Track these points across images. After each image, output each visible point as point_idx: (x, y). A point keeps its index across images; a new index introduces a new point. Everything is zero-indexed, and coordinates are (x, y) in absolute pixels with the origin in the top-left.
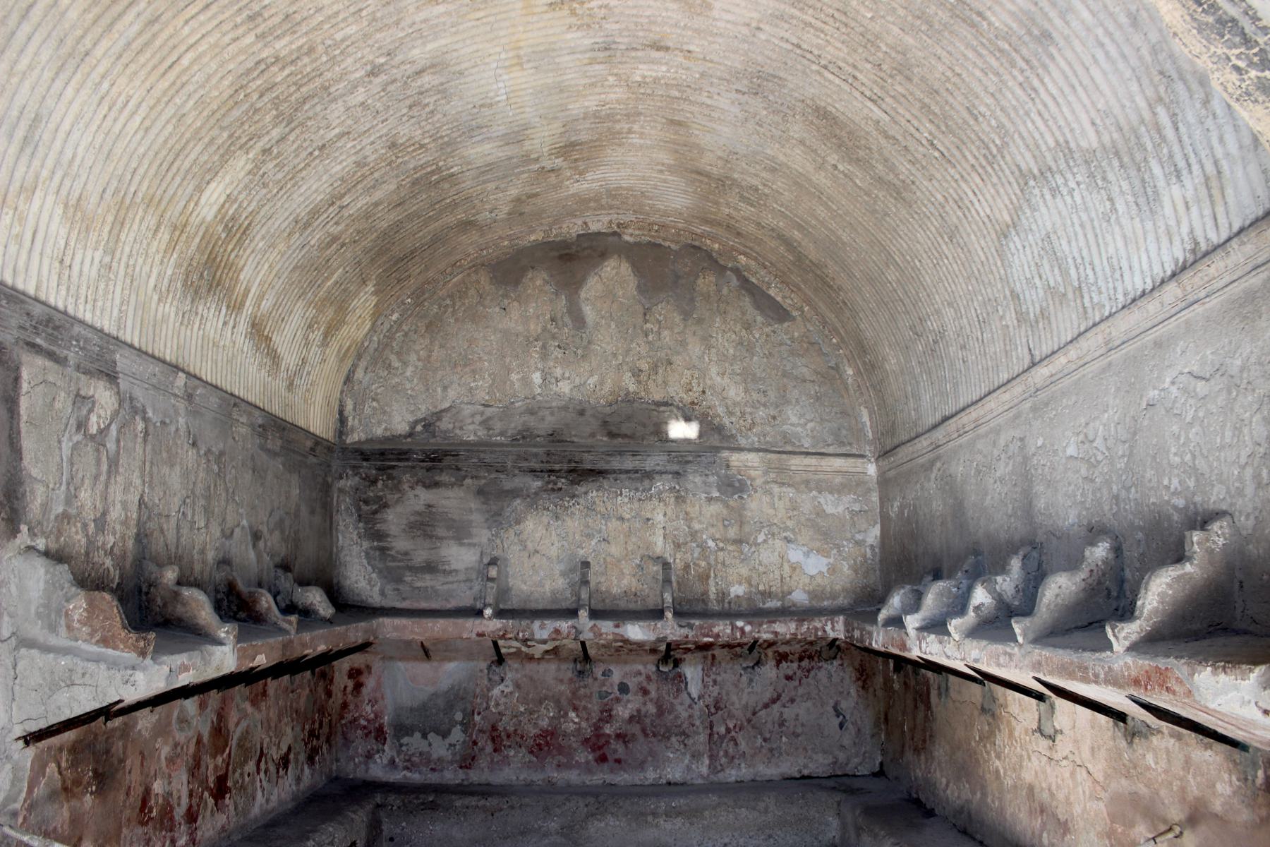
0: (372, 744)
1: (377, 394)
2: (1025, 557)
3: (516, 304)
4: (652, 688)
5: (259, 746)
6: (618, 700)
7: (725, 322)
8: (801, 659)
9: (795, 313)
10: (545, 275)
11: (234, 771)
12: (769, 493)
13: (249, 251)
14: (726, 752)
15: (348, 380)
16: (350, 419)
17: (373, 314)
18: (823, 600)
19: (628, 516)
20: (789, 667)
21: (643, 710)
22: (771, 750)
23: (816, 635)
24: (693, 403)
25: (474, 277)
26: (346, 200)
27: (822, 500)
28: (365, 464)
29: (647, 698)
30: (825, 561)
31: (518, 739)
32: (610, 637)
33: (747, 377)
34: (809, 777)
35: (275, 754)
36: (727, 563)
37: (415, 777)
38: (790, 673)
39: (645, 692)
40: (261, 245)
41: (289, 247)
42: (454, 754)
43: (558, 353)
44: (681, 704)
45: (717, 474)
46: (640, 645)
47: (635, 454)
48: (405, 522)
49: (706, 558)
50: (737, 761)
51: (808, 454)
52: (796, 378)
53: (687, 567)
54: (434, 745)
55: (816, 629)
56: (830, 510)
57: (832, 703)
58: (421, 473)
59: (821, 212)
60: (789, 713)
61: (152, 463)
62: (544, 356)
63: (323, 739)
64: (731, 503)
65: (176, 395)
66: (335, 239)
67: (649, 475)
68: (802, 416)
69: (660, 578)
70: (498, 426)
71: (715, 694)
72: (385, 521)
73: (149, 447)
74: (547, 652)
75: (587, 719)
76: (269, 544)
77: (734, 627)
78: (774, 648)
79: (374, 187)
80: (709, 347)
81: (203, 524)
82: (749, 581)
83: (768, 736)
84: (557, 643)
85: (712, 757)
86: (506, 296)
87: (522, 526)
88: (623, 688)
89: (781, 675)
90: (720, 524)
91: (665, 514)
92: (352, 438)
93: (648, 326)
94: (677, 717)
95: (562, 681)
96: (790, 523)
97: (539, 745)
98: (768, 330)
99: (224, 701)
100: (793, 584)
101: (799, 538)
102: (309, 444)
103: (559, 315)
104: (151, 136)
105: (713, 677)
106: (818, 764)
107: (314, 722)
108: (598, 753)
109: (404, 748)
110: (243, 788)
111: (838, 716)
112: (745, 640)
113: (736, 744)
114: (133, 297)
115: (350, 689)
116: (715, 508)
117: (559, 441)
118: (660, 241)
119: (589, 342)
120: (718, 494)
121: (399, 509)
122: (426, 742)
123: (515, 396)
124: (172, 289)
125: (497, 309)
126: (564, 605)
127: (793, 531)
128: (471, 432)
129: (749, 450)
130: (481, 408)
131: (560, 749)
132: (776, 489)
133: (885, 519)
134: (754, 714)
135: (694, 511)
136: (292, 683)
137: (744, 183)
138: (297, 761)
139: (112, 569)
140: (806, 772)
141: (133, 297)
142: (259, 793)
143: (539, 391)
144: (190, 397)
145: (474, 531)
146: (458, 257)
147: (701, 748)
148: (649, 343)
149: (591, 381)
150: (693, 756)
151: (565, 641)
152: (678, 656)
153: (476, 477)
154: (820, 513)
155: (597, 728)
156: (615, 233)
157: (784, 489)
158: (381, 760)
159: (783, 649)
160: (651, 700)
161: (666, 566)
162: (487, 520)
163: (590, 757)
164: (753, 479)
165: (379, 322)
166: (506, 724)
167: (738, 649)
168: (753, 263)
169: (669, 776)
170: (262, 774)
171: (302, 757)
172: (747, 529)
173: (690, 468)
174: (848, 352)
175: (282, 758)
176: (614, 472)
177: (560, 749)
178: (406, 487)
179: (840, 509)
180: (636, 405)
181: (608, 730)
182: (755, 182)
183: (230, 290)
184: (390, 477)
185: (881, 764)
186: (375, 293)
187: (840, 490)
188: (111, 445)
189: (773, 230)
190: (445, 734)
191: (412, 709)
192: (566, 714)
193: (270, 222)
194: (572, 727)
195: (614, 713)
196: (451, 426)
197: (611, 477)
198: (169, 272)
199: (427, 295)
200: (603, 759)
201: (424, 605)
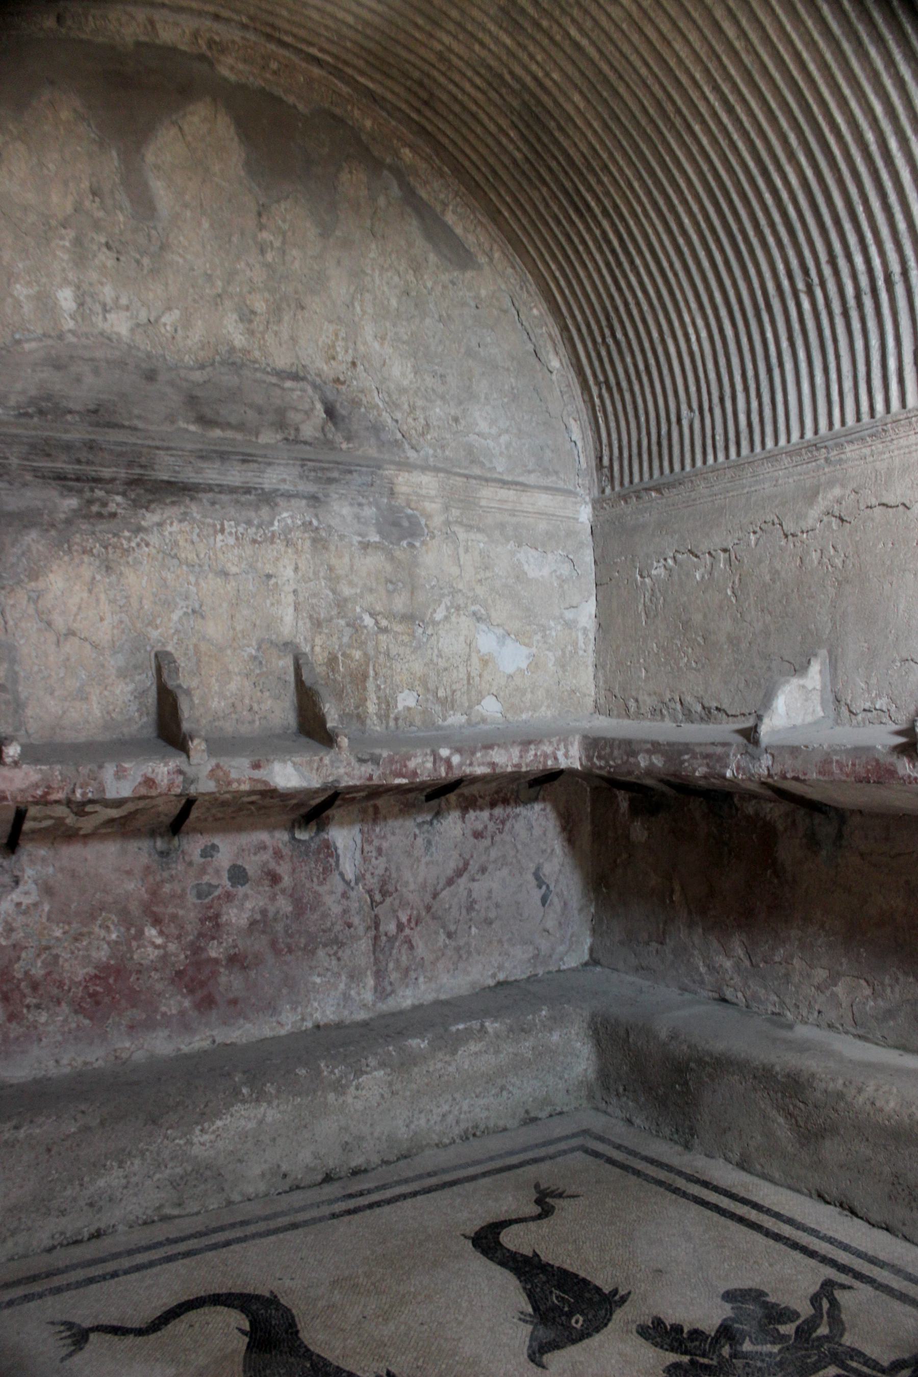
4: (283, 869)
8: (493, 805)
12: (450, 537)
18: (522, 712)
19: (234, 570)
20: (480, 818)
21: (272, 910)
22: (458, 949)
23: (545, 763)
24: (337, 381)
30: (525, 651)
31: (55, 991)
32: (245, 787)
36: (393, 652)
38: (480, 827)
43: (105, 258)
44: (332, 892)
47: (246, 459)
49: (362, 645)
50: (413, 975)
51: (504, 483)
53: (332, 661)
55: (546, 756)
56: (532, 572)
57: (532, 867)
60: (479, 888)
64: (398, 553)
67: (268, 498)
68: (493, 422)
71: (380, 871)
74: (111, 821)
75: (179, 937)
78: (457, 791)
82: (424, 681)
83: (452, 928)
85: (379, 974)
87: (40, 584)
88: (238, 875)
89: (468, 832)
91: (296, 569)
93: (265, 235)
94: (324, 916)
95: (129, 873)
96: (481, 591)
98: (445, 277)
101: (493, 614)
105: (376, 843)
108: (200, 994)
111: (540, 887)
113: (411, 947)
116: (374, 561)
119: (162, 248)
129: (425, 468)
131: (133, 998)
134: (435, 896)
135: (342, 565)
140: (501, 977)
143: (71, 324)
148: (268, 266)
149: (170, 319)
150: (351, 977)
154: (520, 576)
155: (196, 949)
157: (472, 536)
159: (474, 790)
160: (283, 891)
163: (187, 1003)
164: (429, 517)
169: (317, 1015)
174: (556, 331)
176: (209, 488)
177: (133, 998)
179: (546, 572)
180: (246, 372)
181: (214, 951)
185: (591, 950)
192: (140, 934)
194: (153, 954)
195: (224, 919)
197: (206, 497)
200: (207, 1003)
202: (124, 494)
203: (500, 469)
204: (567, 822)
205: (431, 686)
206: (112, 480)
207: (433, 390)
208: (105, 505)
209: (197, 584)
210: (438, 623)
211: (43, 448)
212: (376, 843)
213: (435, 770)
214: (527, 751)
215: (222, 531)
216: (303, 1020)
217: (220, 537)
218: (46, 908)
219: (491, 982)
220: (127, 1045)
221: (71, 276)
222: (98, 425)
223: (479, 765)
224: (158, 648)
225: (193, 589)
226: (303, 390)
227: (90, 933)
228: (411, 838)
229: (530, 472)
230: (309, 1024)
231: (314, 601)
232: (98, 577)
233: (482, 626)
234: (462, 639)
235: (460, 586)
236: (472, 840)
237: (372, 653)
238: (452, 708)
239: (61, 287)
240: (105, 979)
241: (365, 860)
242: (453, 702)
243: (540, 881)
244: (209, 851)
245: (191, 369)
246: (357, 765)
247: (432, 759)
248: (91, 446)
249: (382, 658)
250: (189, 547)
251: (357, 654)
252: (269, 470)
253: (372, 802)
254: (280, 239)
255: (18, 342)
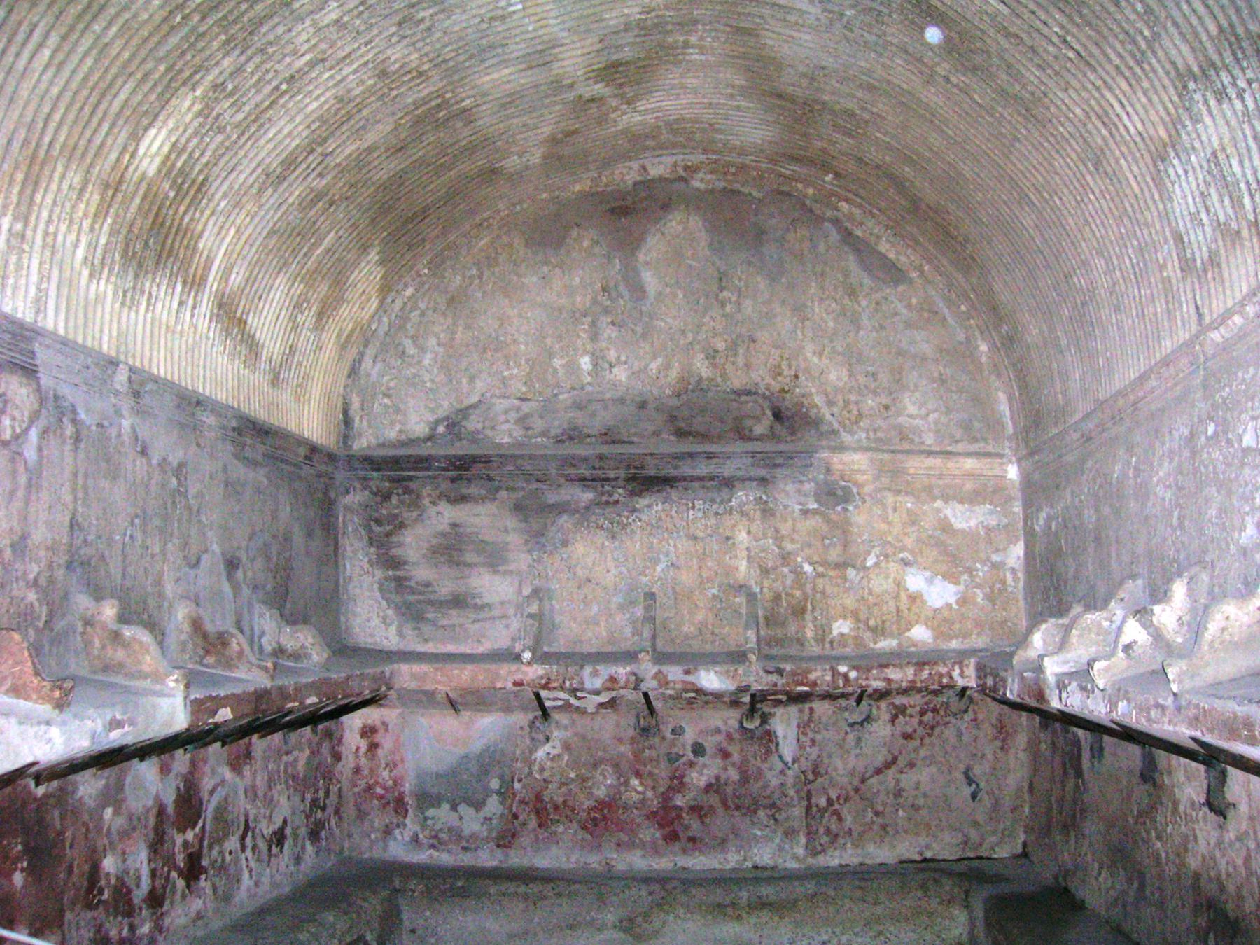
0: (390, 817)
1: (389, 389)
2: (1191, 578)
3: (557, 271)
4: (734, 750)
5: (242, 819)
6: (692, 764)
7: (822, 288)
8: (923, 713)
9: (914, 275)
10: (593, 233)
11: (211, 847)
13: (208, 212)
14: (828, 831)
15: (353, 372)
16: (357, 419)
17: (381, 290)
19: (701, 535)
21: (724, 777)
23: (940, 683)
24: (783, 391)
25: (505, 240)
26: (331, 145)
27: (948, 512)
28: (375, 474)
29: (728, 762)
30: (952, 588)
33: (853, 358)
34: (932, 860)
35: (267, 829)
37: (444, 858)
38: (909, 730)
39: (726, 755)
40: (223, 204)
41: (261, 207)
42: (490, 831)
43: (609, 332)
45: (814, 480)
46: (717, 696)
47: (710, 456)
48: (426, 545)
50: (841, 841)
51: (930, 453)
52: (914, 356)
53: (777, 597)
54: (466, 818)
55: (941, 676)
57: (962, 767)
58: (445, 486)
59: (934, 139)
60: (908, 780)
61: (86, 476)
62: (595, 337)
63: (330, 810)
64: (834, 517)
65: (117, 393)
66: (319, 196)
67: (728, 483)
68: (921, 405)
69: (744, 611)
70: (539, 424)
71: (814, 757)
72: (401, 545)
73: (82, 455)
74: (602, 705)
75: (654, 788)
76: (249, 574)
77: (835, 673)
78: (889, 700)
79: (363, 127)
80: (804, 319)
81: (157, 550)
83: (880, 808)
84: (614, 694)
85: (808, 834)
86: (546, 263)
87: (571, 548)
88: (698, 750)
90: (819, 544)
91: (749, 532)
92: (363, 443)
93: (725, 294)
94: (765, 786)
95: (620, 740)
97: (594, 819)
98: (878, 295)
99: (193, 763)
100: (913, 617)
102: (302, 451)
103: (612, 284)
104: (66, 73)
106: (944, 847)
107: (317, 791)
108: (668, 829)
109: (429, 822)
110: (222, 868)
111: (970, 785)
112: (850, 689)
113: (840, 819)
114: (55, 273)
115: (363, 750)
116: (811, 523)
117: (614, 442)
118: (737, 186)
120: (815, 506)
121: (419, 530)
122: (455, 815)
123: (558, 386)
124: (108, 262)
125: (535, 279)
126: (626, 646)
127: (912, 552)
128: (505, 434)
129: (855, 450)
130: (516, 402)
132: (890, 499)
133: (1030, 535)
134: (863, 781)
135: (785, 529)
136: (286, 743)
137: (837, 107)
138: (296, 837)
139: (36, 604)
140: (929, 854)
141: (55, 273)
142: (246, 875)
143: (589, 379)
144: (136, 395)
145: (511, 556)
146: (485, 215)
147: (796, 824)
149: (654, 366)
151: (622, 692)
152: (766, 710)
153: (513, 489)
154: (946, 527)
155: (666, 798)
156: (681, 179)
157: (899, 498)
158: (401, 838)
159: (899, 700)
161: (751, 597)
162: (527, 541)
163: (658, 835)
165: (389, 300)
166: (554, 794)
167: (843, 702)
168: (856, 211)
169: (757, 858)
170: (249, 853)
171: (303, 831)
172: (853, 550)
173: (779, 473)
175: (275, 833)
176: (685, 479)
178: (426, 502)
180: (710, 394)
181: (679, 801)
182: (851, 105)
183: (186, 263)
184: (407, 491)
185: (1025, 845)
186: (382, 262)
187: (975, 498)
188: (30, 454)
189: (878, 167)
190: (478, 805)
191: (438, 775)
192: (627, 783)
193: (233, 176)
194: (635, 797)
195: (686, 780)
196: (480, 426)
198: (103, 241)
199: (448, 263)
200: (672, 837)
201: (450, 648)
202: (624, 487)
203: (929, 442)
204: (1000, 733)
205: (862, 616)
206: (616, 479)
207: (866, 387)
208: (611, 495)
209: (675, 546)
210: (869, 568)
211: (571, 462)
212: (811, 735)
213: (834, 682)
214: (922, 670)
215: (693, 508)
216: (745, 860)
217: (691, 512)
218: (566, 758)
219: (918, 858)
220: (615, 856)
221: (589, 347)
222: (607, 443)
223: (879, 679)
224: (647, 590)
225: (672, 549)
226: (756, 402)
227: (592, 778)
228: (842, 734)
229: (957, 442)
230: (749, 864)
231: (763, 555)
232: (607, 543)
233: (908, 569)
234: (891, 580)
235: (889, 539)
236: (902, 741)
237: (809, 591)
238: (883, 634)
239: (582, 356)
240: (602, 810)
241: (802, 748)
242: (883, 630)
243: (970, 781)
244: (677, 731)
245: (669, 396)
246: (764, 675)
247: (830, 673)
248: (601, 457)
249: (818, 596)
250: (669, 520)
251: (798, 594)
252: (728, 462)
253: (807, 706)
254: (736, 294)
255: (556, 395)
